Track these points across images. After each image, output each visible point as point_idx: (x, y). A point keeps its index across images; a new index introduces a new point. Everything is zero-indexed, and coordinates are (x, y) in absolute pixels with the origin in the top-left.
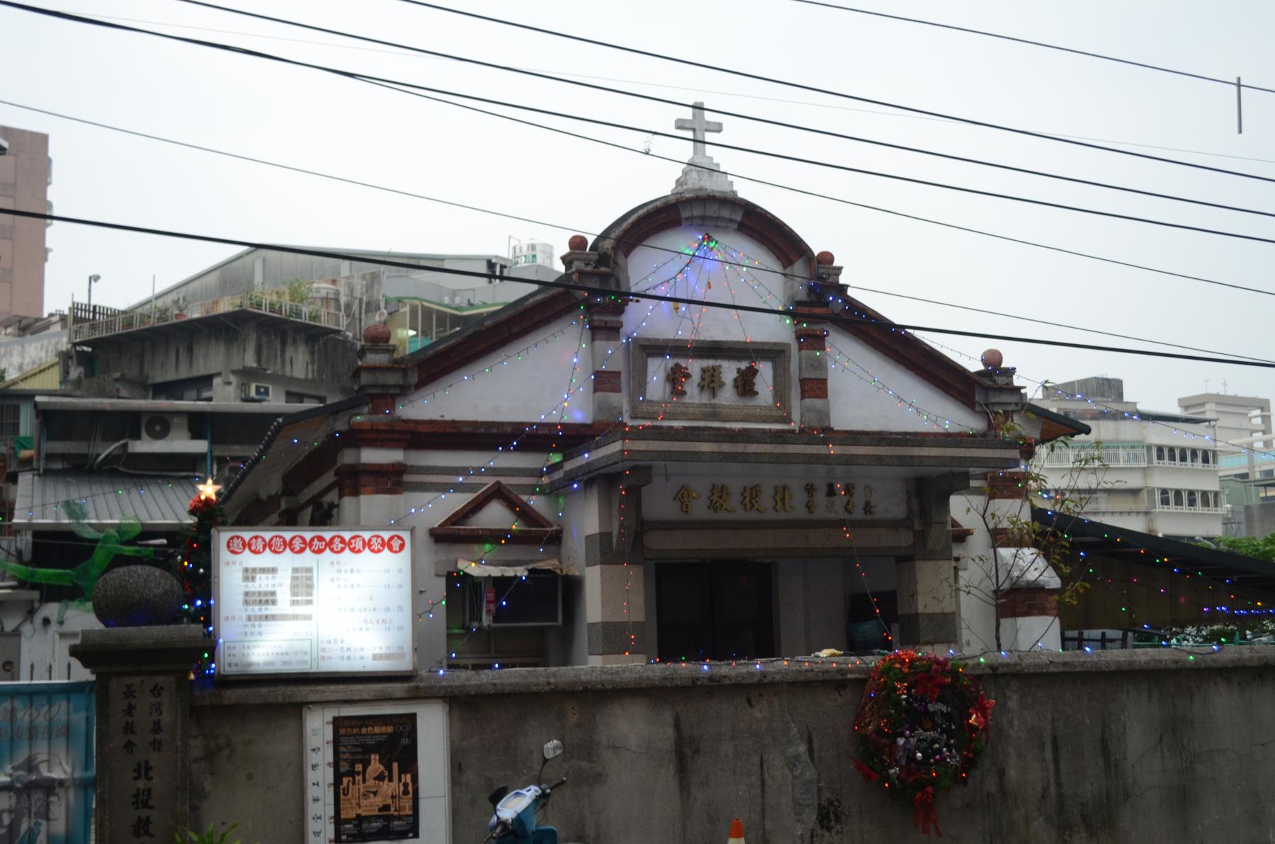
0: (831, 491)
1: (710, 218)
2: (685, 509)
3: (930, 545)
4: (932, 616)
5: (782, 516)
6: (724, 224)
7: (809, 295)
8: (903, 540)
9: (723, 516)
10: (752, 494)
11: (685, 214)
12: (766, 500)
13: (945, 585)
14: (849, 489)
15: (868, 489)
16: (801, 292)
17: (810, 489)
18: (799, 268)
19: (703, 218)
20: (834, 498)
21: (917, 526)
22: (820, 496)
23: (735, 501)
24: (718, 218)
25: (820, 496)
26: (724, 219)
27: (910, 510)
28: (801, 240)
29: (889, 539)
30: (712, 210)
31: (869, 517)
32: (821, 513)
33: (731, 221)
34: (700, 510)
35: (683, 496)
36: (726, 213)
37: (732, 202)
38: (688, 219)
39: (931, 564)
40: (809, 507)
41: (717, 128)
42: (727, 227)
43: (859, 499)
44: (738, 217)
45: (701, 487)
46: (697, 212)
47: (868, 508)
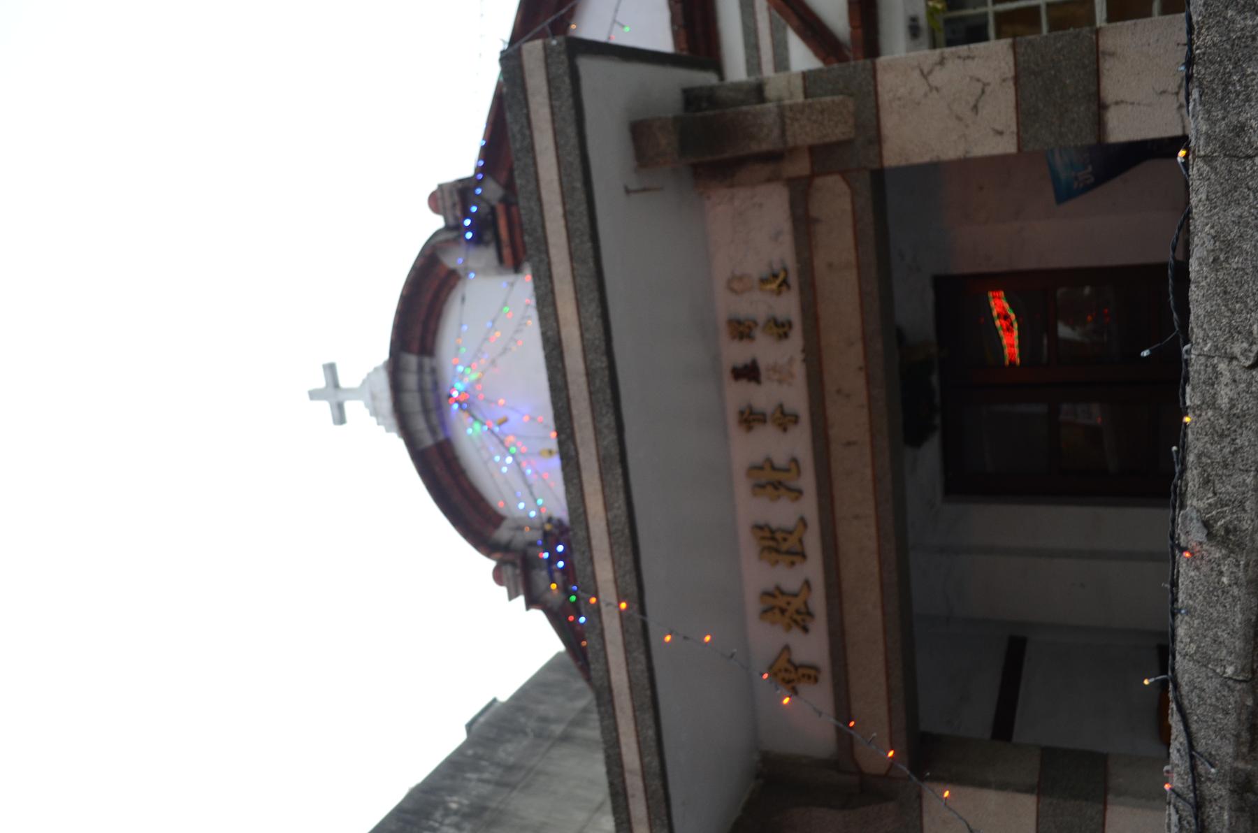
0: (749, 373)
1: (424, 403)
2: (810, 673)
3: (838, 131)
4: (1025, 114)
5: (807, 481)
6: (428, 379)
7: (486, 244)
8: (836, 201)
9: (818, 602)
11: (427, 440)
12: (782, 513)
13: (938, 77)
15: (736, 284)
16: (487, 255)
17: (750, 419)
18: (454, 259)
19: (426, 412)
20: (762, 365)
24: (421, 389)
25: (763, 396)
27: (769, 180)
28: (414, 268)
29: (839, 242)
30: (412, 401)
31: (793, 280)
32: (796, 397)
33: (420, 368)
34: (812, 647)
35: (791, 674)
36: (411, 380)
37: (395, 368)
38: (433, 431)
39: (889, 123)
40: (785, 420)
42: (434, 371)
43: (758, 305)
44: (411, 360)
45: (767, 639)
46: (419, 424)
47: (776, 280)
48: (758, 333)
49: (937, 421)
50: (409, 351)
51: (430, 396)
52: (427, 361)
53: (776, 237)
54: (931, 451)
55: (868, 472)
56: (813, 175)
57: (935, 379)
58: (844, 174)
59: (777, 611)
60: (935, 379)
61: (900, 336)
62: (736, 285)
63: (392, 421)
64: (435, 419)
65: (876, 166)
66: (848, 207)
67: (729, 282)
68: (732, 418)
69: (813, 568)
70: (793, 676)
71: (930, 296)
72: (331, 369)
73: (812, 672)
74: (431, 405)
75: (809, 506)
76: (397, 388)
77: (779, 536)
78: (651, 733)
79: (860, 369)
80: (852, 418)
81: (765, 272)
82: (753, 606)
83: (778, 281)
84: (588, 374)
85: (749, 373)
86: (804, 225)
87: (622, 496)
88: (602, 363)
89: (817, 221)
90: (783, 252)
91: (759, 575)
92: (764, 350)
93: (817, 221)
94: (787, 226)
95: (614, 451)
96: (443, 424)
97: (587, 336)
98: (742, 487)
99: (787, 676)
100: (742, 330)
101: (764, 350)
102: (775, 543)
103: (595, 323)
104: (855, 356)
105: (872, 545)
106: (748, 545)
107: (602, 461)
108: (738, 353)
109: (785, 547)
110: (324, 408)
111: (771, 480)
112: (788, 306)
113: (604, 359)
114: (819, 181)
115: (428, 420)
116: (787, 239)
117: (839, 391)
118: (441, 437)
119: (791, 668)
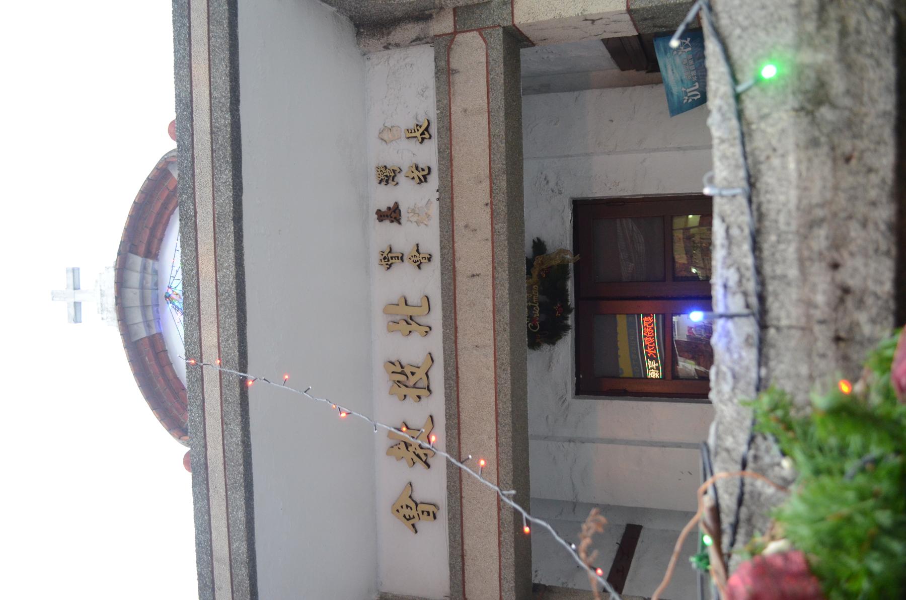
0: (392, 215)
1: (143, 299)
5: (436, 318)
6: (149, 278)
8: (474, 54)
10: (404, 378)
11: (142, 332)
12: (415, 349)
14: (388, 176)
15: (386, 134)
17: (389, 259)
19: (144, 307)
20: (402, 208)
21: (444, 25)
22: (400, 237)
23: (416, 412)
24: (142, 287)
25: (400, 237)
26: (143, 279)
27: (418, 40)
30: (133, 297)
33: (144, 268)
35: (412, 511)
36: (134, 278)
37: (122, 268)
38: (148, 326)
40: (420, 260)
41: (71, 275)
42: (156, 272)
44: (137, 261)
45: (393, 476)
46: (137, 317)
48: (400, 178)
49: (571, 321)
50: (136, 254)
51: (149, 294)
52: (150, 262)
53: (422, 94)
54: (564, 351)
55: (489, 303)
56: (455, 33)
57: (570, 285)
58: (479, 30)
59: (403, 446)
60: (570, 285)
61: (539, 246)
62: (386, 136)
63: (113, 315)
64: (150, 315)
65: (509, 24)
66: (484, 60)
67: (381, 132)
68: (375, 257)
69: (436, 404)
70: (414, 513)
71: (568, 215)
72: (75, 271)
73: (431, 509)
74: (149, 303)
75: (435, 343)
76: (121, 284)
77: (408, 371)
78: (241, 514)
79: (487, 204)
80: (478, 252)
81: (412, 126)
82: (382, 443)
83: (421, 130)
84: (212, 133)
85: (392, 215)
86: (445, 74)
87: (232, 254)
88: (225, 119)
89: (456, 71)
90: (426, 108)
91: (391, 411)
92: (407, 194)
93: (456, 71)
94: (431, 82)
95: (229, 208)
96: (158, 320)
97: (215, 94)
98: (380, 321)
99: (408, 512)
100: (388, 176)
101: (407, 194)
102: (404, 378)
103: (223, 83)
104: (482, 193)
105: (490, 375)
106: (382, 380)
107: (216, 218)
108: (384, 197)
109: (412, 380)
110: (64, 309)
111: (406, 318)
112: (427, 154)
113: (228, 116)
114: (459, 38)
115: (144, 315)
116: (431, 93)
117: (466, 226)
118: (154, 331)
119: (413, 506)
